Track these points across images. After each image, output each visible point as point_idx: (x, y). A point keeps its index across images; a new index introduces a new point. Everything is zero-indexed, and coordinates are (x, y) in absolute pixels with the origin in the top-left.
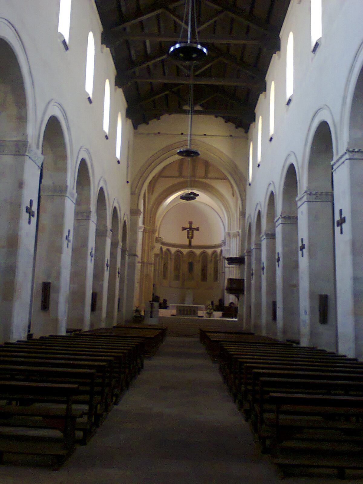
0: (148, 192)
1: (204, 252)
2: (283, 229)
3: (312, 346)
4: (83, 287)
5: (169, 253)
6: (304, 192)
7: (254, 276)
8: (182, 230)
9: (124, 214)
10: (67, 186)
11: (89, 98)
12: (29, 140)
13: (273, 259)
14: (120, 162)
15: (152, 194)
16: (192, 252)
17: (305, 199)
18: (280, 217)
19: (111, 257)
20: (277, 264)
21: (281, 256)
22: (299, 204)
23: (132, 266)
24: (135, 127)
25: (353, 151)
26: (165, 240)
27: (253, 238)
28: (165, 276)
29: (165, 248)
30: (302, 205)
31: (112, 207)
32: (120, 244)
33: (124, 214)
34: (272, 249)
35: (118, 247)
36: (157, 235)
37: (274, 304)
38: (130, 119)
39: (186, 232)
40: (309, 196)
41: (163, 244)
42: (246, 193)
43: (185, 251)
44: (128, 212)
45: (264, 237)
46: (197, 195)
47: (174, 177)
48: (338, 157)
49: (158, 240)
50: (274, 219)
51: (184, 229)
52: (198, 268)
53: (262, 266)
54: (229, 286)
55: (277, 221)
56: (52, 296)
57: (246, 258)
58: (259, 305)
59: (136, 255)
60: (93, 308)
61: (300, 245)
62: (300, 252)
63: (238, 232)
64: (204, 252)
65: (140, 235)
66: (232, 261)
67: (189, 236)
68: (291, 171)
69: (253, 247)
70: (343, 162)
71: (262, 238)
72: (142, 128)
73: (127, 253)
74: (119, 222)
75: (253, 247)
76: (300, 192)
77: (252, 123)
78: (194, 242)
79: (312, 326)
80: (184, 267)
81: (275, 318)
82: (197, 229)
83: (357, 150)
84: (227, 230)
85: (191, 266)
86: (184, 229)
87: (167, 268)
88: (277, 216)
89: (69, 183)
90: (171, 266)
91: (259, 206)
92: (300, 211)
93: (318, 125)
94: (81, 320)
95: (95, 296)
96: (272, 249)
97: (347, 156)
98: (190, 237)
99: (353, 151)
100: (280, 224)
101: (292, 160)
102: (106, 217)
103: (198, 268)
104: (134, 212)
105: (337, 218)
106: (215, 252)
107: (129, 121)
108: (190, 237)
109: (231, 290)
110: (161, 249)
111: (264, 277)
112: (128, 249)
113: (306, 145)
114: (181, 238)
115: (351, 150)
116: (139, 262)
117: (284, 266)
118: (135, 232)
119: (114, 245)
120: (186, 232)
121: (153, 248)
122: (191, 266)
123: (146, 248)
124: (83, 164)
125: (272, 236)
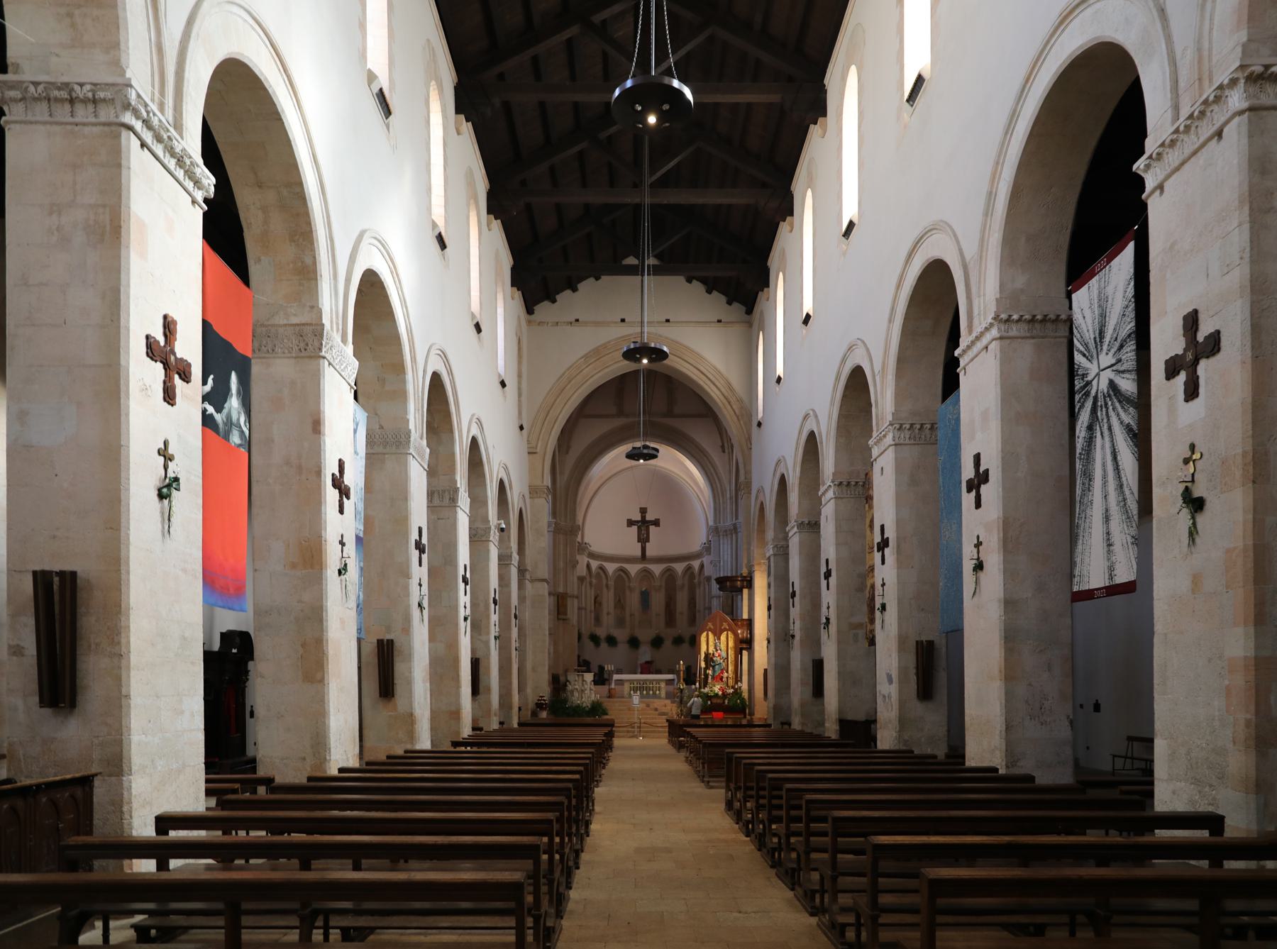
1: (668, 570)
8: (628, 526)
22: (875, 452)
29: (595, 564)
30: (879, 456)
32: (515, 557)
36: (579, 539)
41: (592, 556)
43: (633, 569)
49: (583, 547)
51: (630, 523)
55: (824, 494)
68: (857, 383)
71: (789, 531)
80: (633, 600)
85: (645, 597)
86: (630, 523)
90: (609, 599)
96: (812, 553)
100: (832, 499)
103: (658, 600)
106: (689, 568)
110: (588, 566)
121: (575, 564)
123: (562, 565)
125: (812, 526)
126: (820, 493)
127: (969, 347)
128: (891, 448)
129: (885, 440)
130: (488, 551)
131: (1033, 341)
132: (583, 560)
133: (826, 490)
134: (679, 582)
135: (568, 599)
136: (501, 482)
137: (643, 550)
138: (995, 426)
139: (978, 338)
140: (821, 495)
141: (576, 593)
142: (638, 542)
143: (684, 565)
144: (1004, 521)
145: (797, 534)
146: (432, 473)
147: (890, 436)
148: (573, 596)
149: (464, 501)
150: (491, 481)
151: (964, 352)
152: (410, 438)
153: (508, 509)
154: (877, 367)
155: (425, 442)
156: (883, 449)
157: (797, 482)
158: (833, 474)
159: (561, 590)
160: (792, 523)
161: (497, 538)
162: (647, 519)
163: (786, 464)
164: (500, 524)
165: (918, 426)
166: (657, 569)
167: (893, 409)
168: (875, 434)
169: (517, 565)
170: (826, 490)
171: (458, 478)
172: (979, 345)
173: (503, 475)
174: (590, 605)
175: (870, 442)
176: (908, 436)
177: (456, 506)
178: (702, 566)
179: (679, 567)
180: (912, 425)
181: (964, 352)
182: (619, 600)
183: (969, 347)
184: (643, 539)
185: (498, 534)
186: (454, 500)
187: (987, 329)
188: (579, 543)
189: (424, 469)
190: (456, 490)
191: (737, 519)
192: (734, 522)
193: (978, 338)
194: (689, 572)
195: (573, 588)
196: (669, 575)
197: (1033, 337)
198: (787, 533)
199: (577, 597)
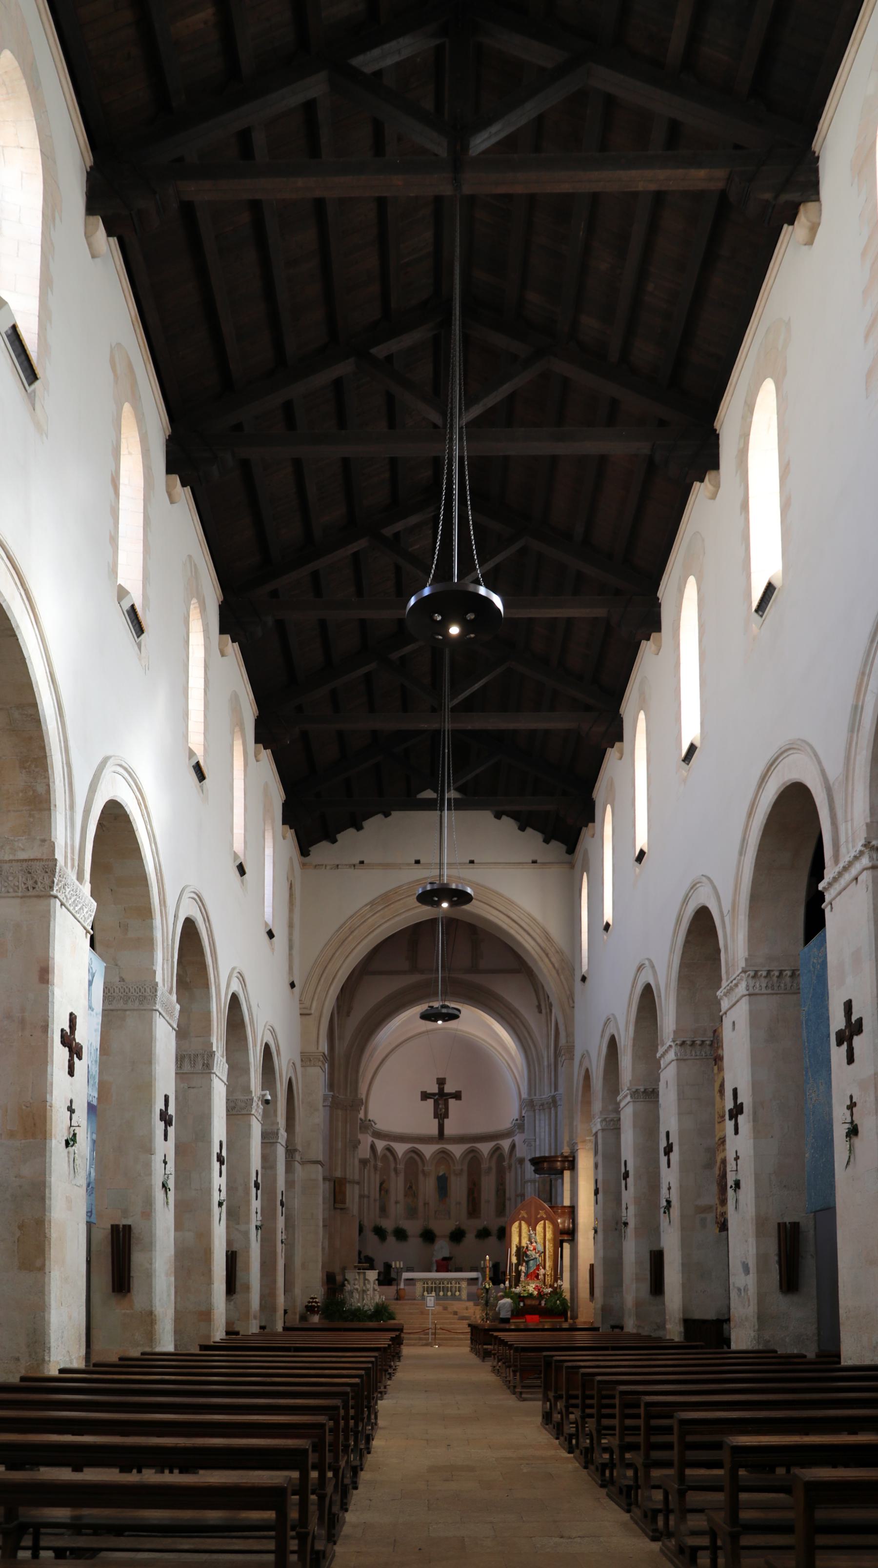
1: (472, 1151)
2: (678, 1074)
6: (740, 970)
8: (422, 1100)
16: (444, 1152)
19: (263, 1167)
22: (725, 1004)
32: (283, 1135)
36: (361, 1115)
43: (428, 1150)
49: (366, 1125)
50: (656, 1051)
51: (425, 1096)
53: (623, 1170)
55: (663, 1056)
71: (621, 1101)
76: (727, 972)
86: (425, 1096)
91: (612, 1024)
93: (775, 797)
100: (673, 1061)
101: (703, 897)
103: (458, 1187)
113: (742, 852)
117: (682, 1163)
121: (356, 1144)
123: (340, 1145)
126: (658, 1055)
127: (835, 880)
128: (744, 999)
129: (737, 990)
130: (249, 1126)
132: (366, 1140)
133: (666, 1051)
134: (484, 1166)
135: (348, 1185)
136: (267, 1047)
139: (846, 869)
140: (660, 1057)
141: (357, 1178)
142: (435, 1117)
143: (492, 1144)
145: (631, 1104)
146: (182, 1034)
147: (743, 985)
148: (353, 1182)
149: (220, 1067)
150: (255, 1045)
151: (830, 884)
152: (156, 991)
153: (275, 1078)
154: (727, 906)
155: (174, 997)
156: (734, 1000)
157: (630, 1043)
158: (674, 1032)
161: (260, 1111)
163: (616, 1022)
164: (264, 1096)
165: (777, 973)
167: (747, 954)
168: (724, 984)
169: (284, 1144)
170: (666, 1051)
171: (214, 1040)
172: (848, 877)
174: (375, 1193)
175: (719, 993)
176: (764, 985)
177: (211, 1073)
178: (513, 1147)
180: (769, 972)
181: (830, 884)
182: (411, 1187)
183: (835, 880)
184: (441, 1115)
185: (261, 1107)
186: (208, 1067)
187: (856, 858)
188: (361, 1120)
189: (173, 1028)
190: (212, 1054)
191: (556, 1089)
192: (553, 1093)
193: (846, 869)
194: (497, 1153)
195: (353, 1171)
196: (473, 1159)
199: (358, 1183)
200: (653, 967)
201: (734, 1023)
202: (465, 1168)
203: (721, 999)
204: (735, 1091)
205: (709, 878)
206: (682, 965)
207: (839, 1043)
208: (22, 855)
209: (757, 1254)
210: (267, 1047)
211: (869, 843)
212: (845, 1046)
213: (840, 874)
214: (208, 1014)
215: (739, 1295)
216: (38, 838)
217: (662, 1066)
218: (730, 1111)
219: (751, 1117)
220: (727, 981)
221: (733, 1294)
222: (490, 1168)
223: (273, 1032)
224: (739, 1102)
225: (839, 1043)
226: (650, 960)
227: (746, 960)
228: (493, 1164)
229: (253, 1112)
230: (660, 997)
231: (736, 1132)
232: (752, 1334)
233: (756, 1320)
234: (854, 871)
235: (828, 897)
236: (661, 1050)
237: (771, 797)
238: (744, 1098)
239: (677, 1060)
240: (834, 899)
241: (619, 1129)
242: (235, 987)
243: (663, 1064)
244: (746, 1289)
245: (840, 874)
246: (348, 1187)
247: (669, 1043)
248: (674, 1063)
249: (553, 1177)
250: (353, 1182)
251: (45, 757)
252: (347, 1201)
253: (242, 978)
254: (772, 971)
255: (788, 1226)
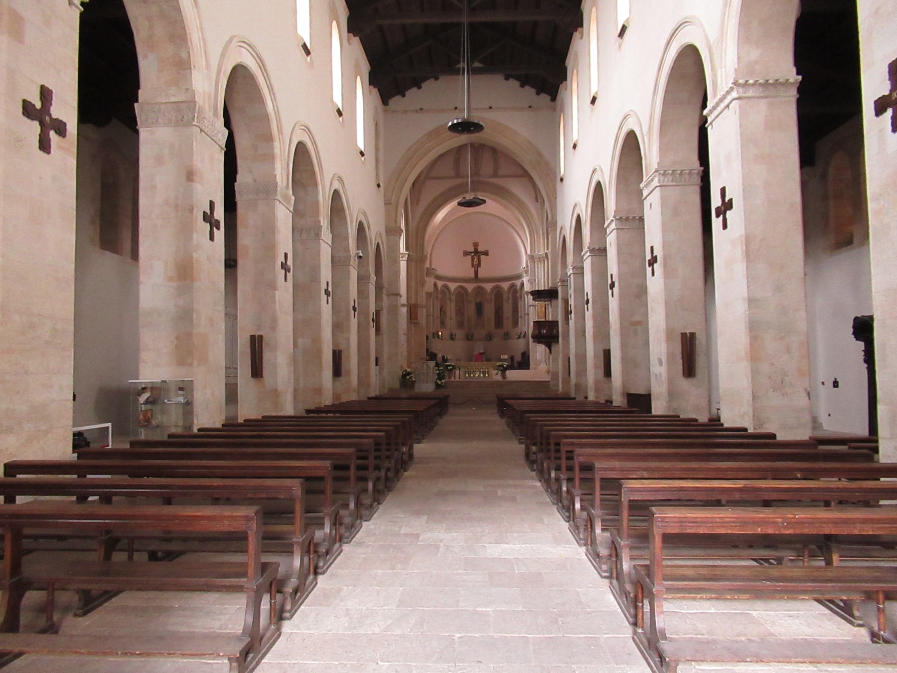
0: (411, 203)
2: (618, 238)
3: (671, 413)
4: (317, 340)
5: (446, 290)
6: (654, 170)
7: (573, 315)
9: (376, 230)
10: (275, 185)
11: (304, 46)
12: (199, 99)
13: (604, 284)
14: (365, 153)
15: (417, 205)
16: (479, 287)
17: (656, 182)
18: (613, 219)
20: (610, 291)
21: (615, 279)
22: (645, 193)
23: (394, 309)
24: (385, 100)
25: (746, 85)
26: (440, 272)
27: (570, 258)
28: (443, 323)
29: (440, 284)
30: (650, 194)
31: (357, 221)
32: (373, 277)
33: (376, 230)
34: (601, 270)
35: (369, 282)
37: (607, 354)
38: (375, 87)
39: (469, 258)
40: (662, 178)
42: (556, 194)
43: (470, 287)
44: (382, 230)
45: (588, 254)
46: (484, 202)
47: (447, 178)
48: (716, 100)
49: (430, 272)
50: (604, 223)
52: (489, 310)
54: (537, 332)
55: (608, 226)
56: (267, 355)
57: (560, 290)
58: (581, 358)
59: (398, 295)
60: (337, 371)
61: (648, 257)
62: (649, 270)
63: (546, 254)
64: (498, 287)
65: (403, 265)
66: (538, 295)
67: (475, 264)
69: (570, 271)
70: (728, 106)
72: (396, 102)
73: (384, 292)
74: (370, 248)
75: (570, 271)
76: (646, 172)
77: (562, 83)
78: (482, 273)
79: (671, 381)
80: (471, 309)
81: (608, 373)
82: (486, 253)
83: (751, 82)
84: (529, 253)
85: (479, 308)
87: (445, 312)
88: (608, 219)
89: (279, 179)
90: (451, 308)
92: (646, 204)
93: (676, 55)
94: (318, 391)
95: (337, 356)
96: (601, 270)
97: (734, 94)
98: (477, 266)
99: (746, 85)
100: (614, 229)
102: (348, 237)
103: (489, 310)
104: (392, 231)
105: (716, 201)
106: (513, 285)
107: (375, 91)
108: (477, 266)
109: (538, 338)
110: (435, 285)
111: (589, 314)
112: (385, 285)
114: (464, 269)
115: (741, 81)
116: (403, 305)
118: (395, 262)
119: (362, 280)
120: (469, 258)
121: (423, 284)
122: (479, 308)
123: (413, 284)
124: (301, 151)
125: (600, 252)
126: (605, 226)
127: (714, 108)
129: (652, 183)
131: (767, 100)
132: (430, 282)
133: (610, 224)
134: (505, 297)
135: (419, 309)
136: (361, 224)
137: (476, 273)
138: (737, 165)
139: (721, 100)
141: (424, 303)
144: (746, 238)
145: (590, 257)
148: (422, 307)
149: (326, 235)
150: (352, 221)
154: (645, 129)
155: (291, 192)
156: (651, 189)
158: (615, 211)
159: (413, 302)
160: (585, 249)
161: (357, 263)
162: (479, 250)
163: (580, 206)
164: (358, 253)
166: (488, 287)
168: (644, 179)
169: (374, 283)
170: (610, 224)
172: (722, 105)
173: (362, 218)
174: (438, 313)
175: (642, 185)
178: (523, 284)
179: (505, 285)
180: (674, 171)
181: (711, 112)
183: (714, 108)
186: (318, 235)
187: (728, 93)
190: (320, 228)
195: (423, 300)
197: (767, 97)
198: (583, 257)
199: (426, 307)
200: (602, 170)
201: (651, 204)
202: (493, 297)
203: (643, 189)
204: (652, 248)
205: (635, 112)
206: (619, 168)
207: (718, 216)
208: (173, 99)
209: (668, 353)
210: (361, 224)
211: (737, 81)
212: (721, 217)
213: (717, 104)
214: (317, 202)
215: (656, 379)
216: (184, 87)
217: (608, 232)
218: (649, 260)
219: (662, 265)
220: (646, 176)
221: (653, 379)
222: (508, 298)
223: (365, 214)
224: (654, 255)
225: (718, 216)
226: (600, 167)
227: (658, 163)
228: (510, 296)
229: (351, 263)
230: (606, 189)
231: (653, 275)
232: (665, 404)
233: (667, 395)
234: (726, 102)
235: (709, 120)
236: (607, 223)
237: (673, 56)
238: (658, 252)
239: (617, 229)
240: (712, 121)
241: (583, 273)
242: (337, 185)
243: (608, 231)
244: (661, 375)
245: (717, 104)
246: (419, 310)
247: (612, 218)
248: (615, 231)
249: (547, 302)
250: (422, 307)
251: (185, 34)
252: (419, 318)
253: (340, 179)
254: (676, 170)
255: (688, 335)
